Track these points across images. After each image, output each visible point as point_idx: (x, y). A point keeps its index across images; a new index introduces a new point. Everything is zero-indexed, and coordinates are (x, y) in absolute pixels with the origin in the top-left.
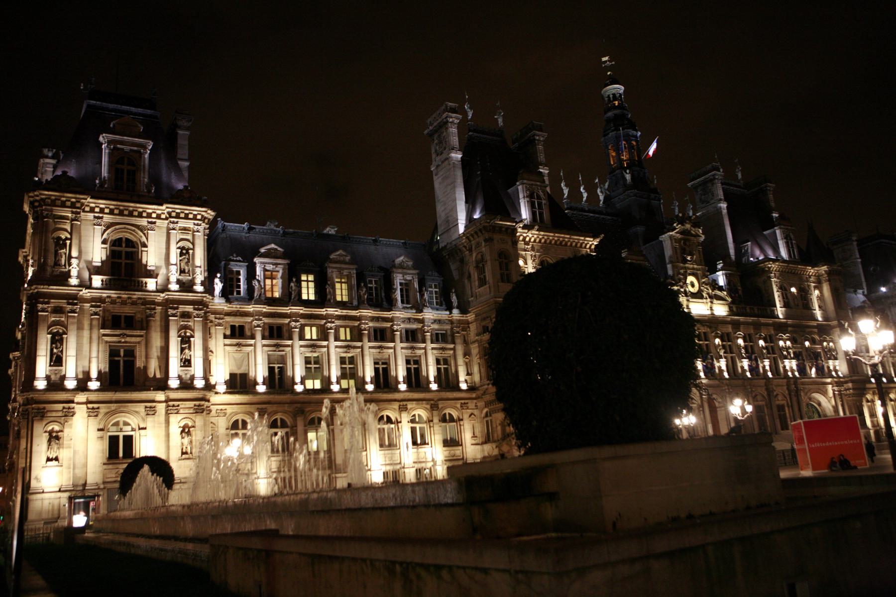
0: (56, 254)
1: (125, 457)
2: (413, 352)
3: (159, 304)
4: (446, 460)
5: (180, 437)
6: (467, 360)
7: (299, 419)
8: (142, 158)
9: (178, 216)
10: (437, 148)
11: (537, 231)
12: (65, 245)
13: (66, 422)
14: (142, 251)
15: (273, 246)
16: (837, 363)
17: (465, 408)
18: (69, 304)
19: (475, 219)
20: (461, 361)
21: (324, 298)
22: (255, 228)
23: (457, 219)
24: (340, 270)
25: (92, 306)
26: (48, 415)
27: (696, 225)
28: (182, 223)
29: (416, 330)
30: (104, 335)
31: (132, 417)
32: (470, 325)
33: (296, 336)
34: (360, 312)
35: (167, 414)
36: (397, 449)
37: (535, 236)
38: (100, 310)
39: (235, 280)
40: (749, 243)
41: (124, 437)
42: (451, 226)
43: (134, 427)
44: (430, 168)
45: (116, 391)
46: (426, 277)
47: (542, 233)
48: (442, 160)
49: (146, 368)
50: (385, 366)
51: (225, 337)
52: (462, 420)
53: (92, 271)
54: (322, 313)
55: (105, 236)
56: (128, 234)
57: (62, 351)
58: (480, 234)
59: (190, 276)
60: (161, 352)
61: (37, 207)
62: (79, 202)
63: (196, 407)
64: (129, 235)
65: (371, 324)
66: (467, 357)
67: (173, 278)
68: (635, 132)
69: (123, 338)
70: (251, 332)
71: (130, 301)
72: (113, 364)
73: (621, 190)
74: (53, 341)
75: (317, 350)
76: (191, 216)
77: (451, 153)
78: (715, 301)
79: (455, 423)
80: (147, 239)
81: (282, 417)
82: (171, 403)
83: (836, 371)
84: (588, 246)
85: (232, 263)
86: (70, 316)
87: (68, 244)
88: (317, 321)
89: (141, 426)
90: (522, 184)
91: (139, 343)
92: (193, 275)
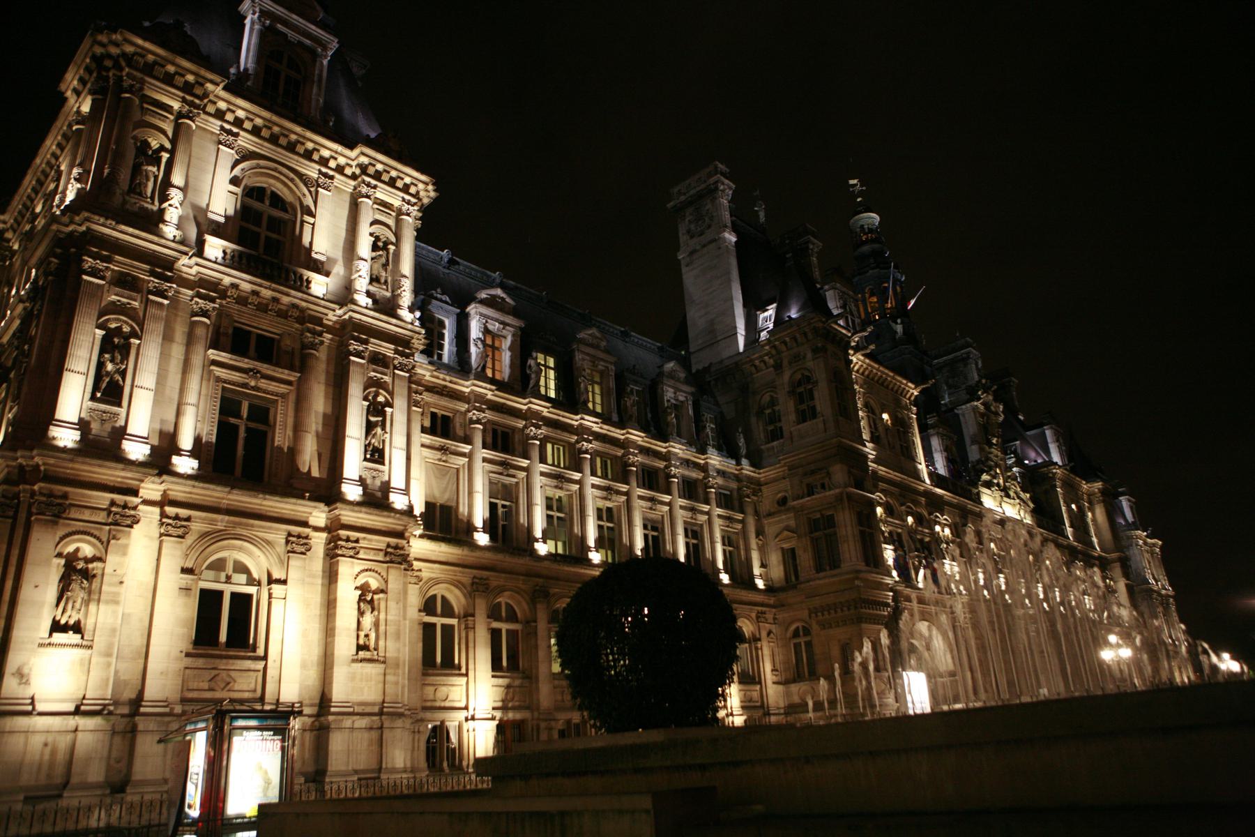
0: (137, 170)
1: (231, 643)
3: (330, 330)
5: (356, 612)
6: (760, 542)
7: (539, 606)
8: (318, 64)
9: (377, 176)
10: (692, 227)
11: (863, 355)
12: (157, 162)
13: (114, 538)
15: (499, 292)
18: (153, 273)
20: (753, 542)
21: (570, 399)
22: (458, 263)
23: (736, 327)
24: (594, 360)
25: (199, 295)
26: (72, 516)
28: (383, 193)
29: (696, 480)
30: (214, 363)
32: (763, 488)
33: (535, 454)
35: (332, 555)
37: (860, 363)
38: (214, 308)
39: (436, 333)
40: (1018, 442)
41: (234, 595)
42: (719, 338)
43: (256, 575)
44: (676, 256)
45: (233, 488)
46: (701, 402)
47: (867, 361)
49: (293, 452)
50: (655, 534)
51: (424, 430)
52: (759, 640)
55: (237, 171)
57: (123, 374)
59: (387, 290)
60: (324, 425)
61: (108, 70)
63: (389, 550)
65: (640, 459)
66: (761, 537)
67: (362, 284)
69: (256, 378)
70: (465, 431)
72: (225, 430)
74: (107, 346)
75: (566, 485)
76: (400, 184)
77: (724, 231)
79: (747, 645)
80: (315, 203)
81: (510, 602)
82: (343, 533)
85: (434, 302)
86: (153, 302)
87: (164, 160)
88: (566, 434)
89: (276, 576)
90: (834, 288)
91: (283, 396)
92: (393, 291)
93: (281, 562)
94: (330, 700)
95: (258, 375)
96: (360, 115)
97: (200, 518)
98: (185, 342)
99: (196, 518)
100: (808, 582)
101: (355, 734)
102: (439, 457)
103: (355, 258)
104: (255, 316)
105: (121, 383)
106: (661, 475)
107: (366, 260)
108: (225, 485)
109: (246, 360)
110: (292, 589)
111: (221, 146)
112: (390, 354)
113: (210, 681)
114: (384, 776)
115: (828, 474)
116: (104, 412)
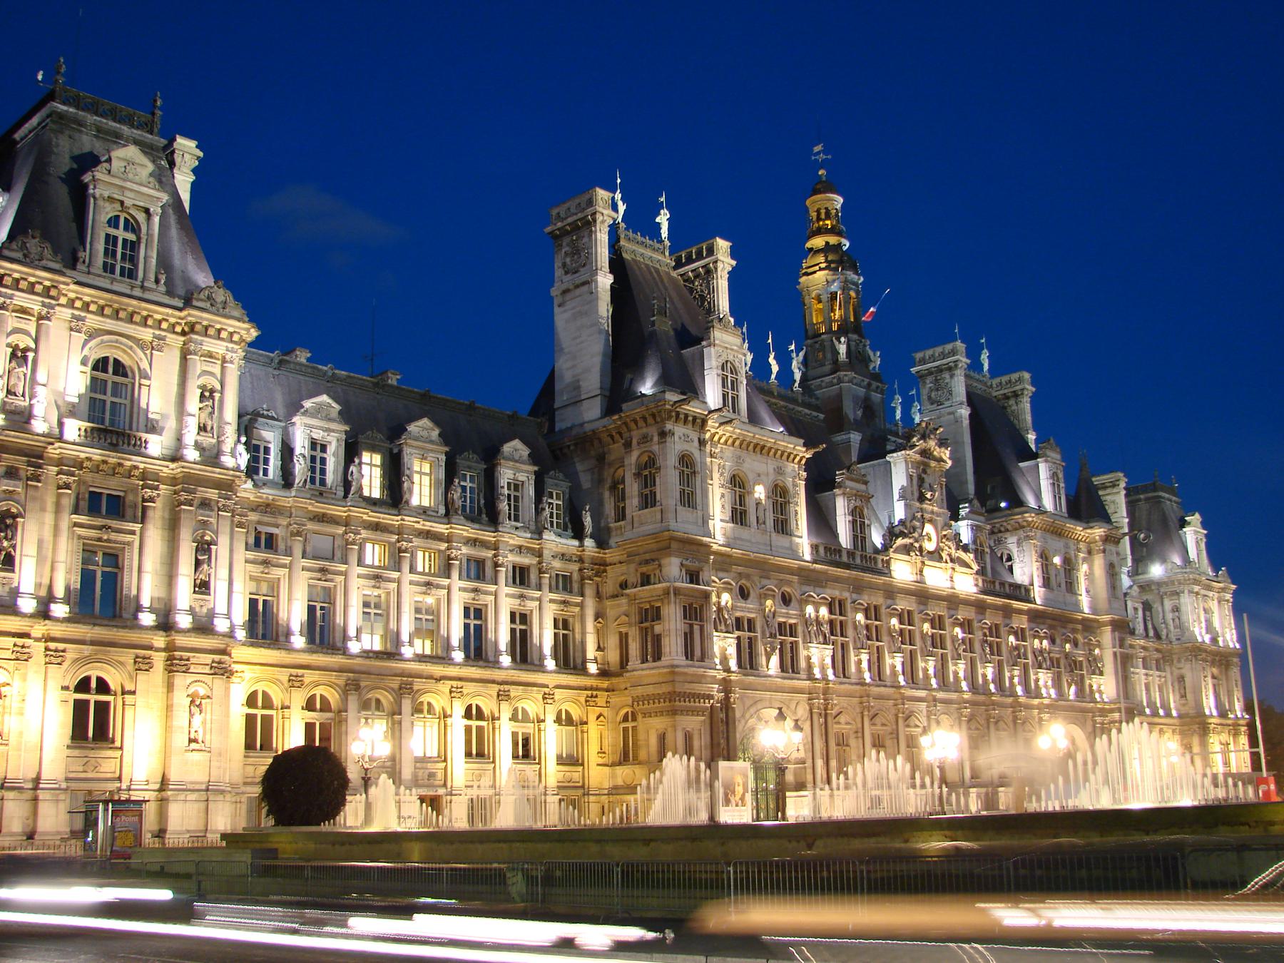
2: (522, 604)
4: (559, 787)
7: (350, 698)
10: (568, 260)
14: (140, 385)
15: (324, 398)
16: (1102, 680)
17: (592, 704)
18: (30, 464)
19: (644, 395)
27: (942, 443)
28: (210, 345)
30: (76, 525)
31: (115, 671)
34: (451, 528)
36: (488, 763)
37: (728, 434)
42: (583, 397)
45: (95, 625)
48: (578, 282)
52: (586, 723)
53: (63, 409)
54: (395, 523)
56: (119, 353)
57: (14, 547)
58: (650, 420)
62: (56, 287)
64: (121, 354)
65: (465, 550)
66: (600, 620)
67: (191, 436)
68: (857, 277)
69: (107, 533)
73: (828, 368)
75: (383, 584)
78: (957, 567)
83: (1100, 692)
84: (796, 460)
86: (31, 485)
89: (127, 688)
93: (131, 677)
94: (169, 780)
96: (190, 258)
97: (72, 649)
98: (54, 510)
100: (633, 671)
101: (188, 804)
102: (262, 570)
103: (185, 414)
105: (13, 553)
106: (489, 565)
107: (194, 416)
108: (89, 624)
110: (139, 699)
111: (72, 333)
112: (215, 497)
114: (208, 835)
115: (660, 565)
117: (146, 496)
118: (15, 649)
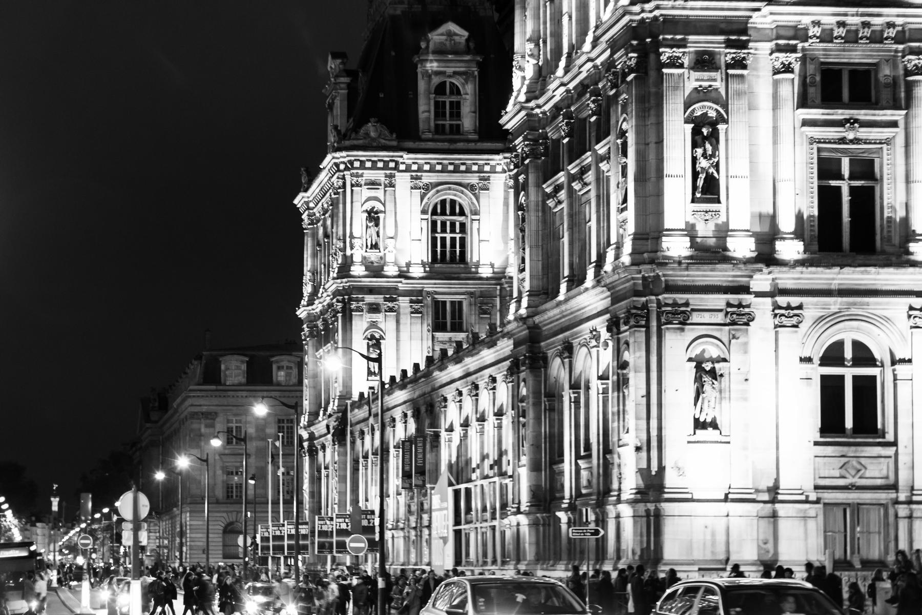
13: (734, 337)
18: (729, 44)
25: (779, 49)
26: (694, 321)
30: (806, 123)
57: (717, 166)
69: (853, 129)
71: (867, 32)
74: (697, 140)
86: (733, 76)
91: (888, 142)
95: (856, 125)
99: (807, 304)
104: (844, 50)
105: (716, 175)
109: (840, 111)
113: (841, 468)
116: (707, 212)
117: (910, 66)
118: (729, 310)
